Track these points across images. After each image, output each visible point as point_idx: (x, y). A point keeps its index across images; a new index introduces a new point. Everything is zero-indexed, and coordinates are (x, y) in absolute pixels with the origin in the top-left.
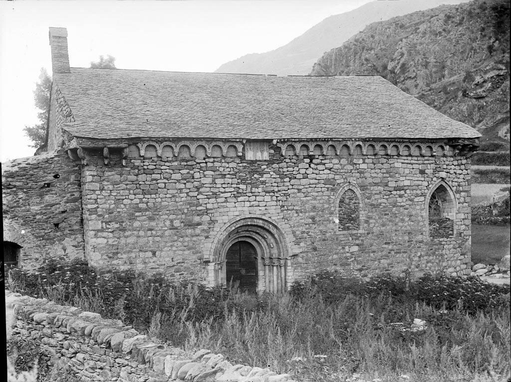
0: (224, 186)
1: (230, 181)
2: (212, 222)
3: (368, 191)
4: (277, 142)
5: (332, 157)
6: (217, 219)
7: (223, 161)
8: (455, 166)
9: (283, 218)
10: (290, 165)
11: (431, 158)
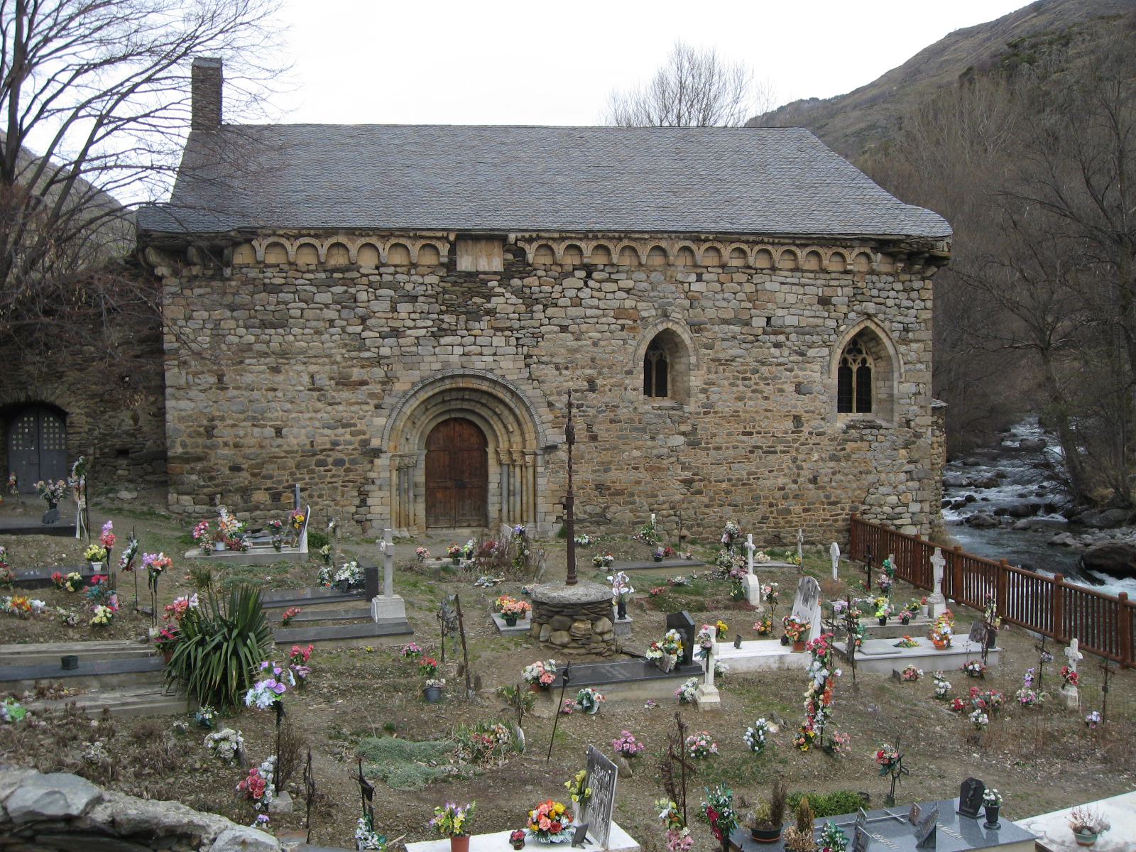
0: (413, 316)
1: (426, 308)
2: (388, 381)
3: (706, 333)
4: (517, 240)
5: (633, 269)
7: (413, 271)
8: (897, 292)
9: (528, 379)
10: (546, 281)
11: (843, 276)
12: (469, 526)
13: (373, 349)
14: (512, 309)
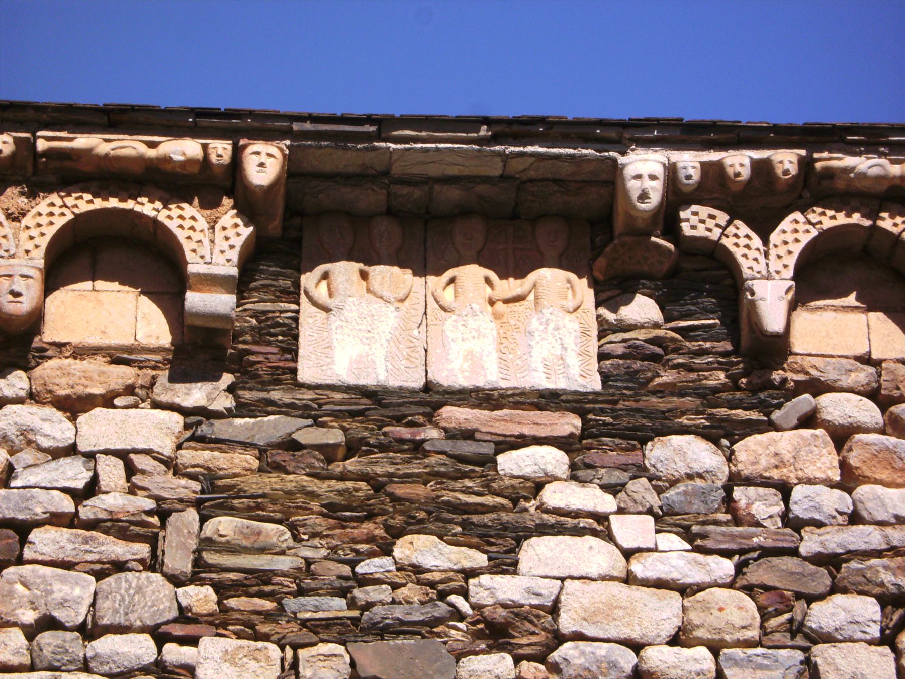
4: (677, 195)
14: (666, 612)
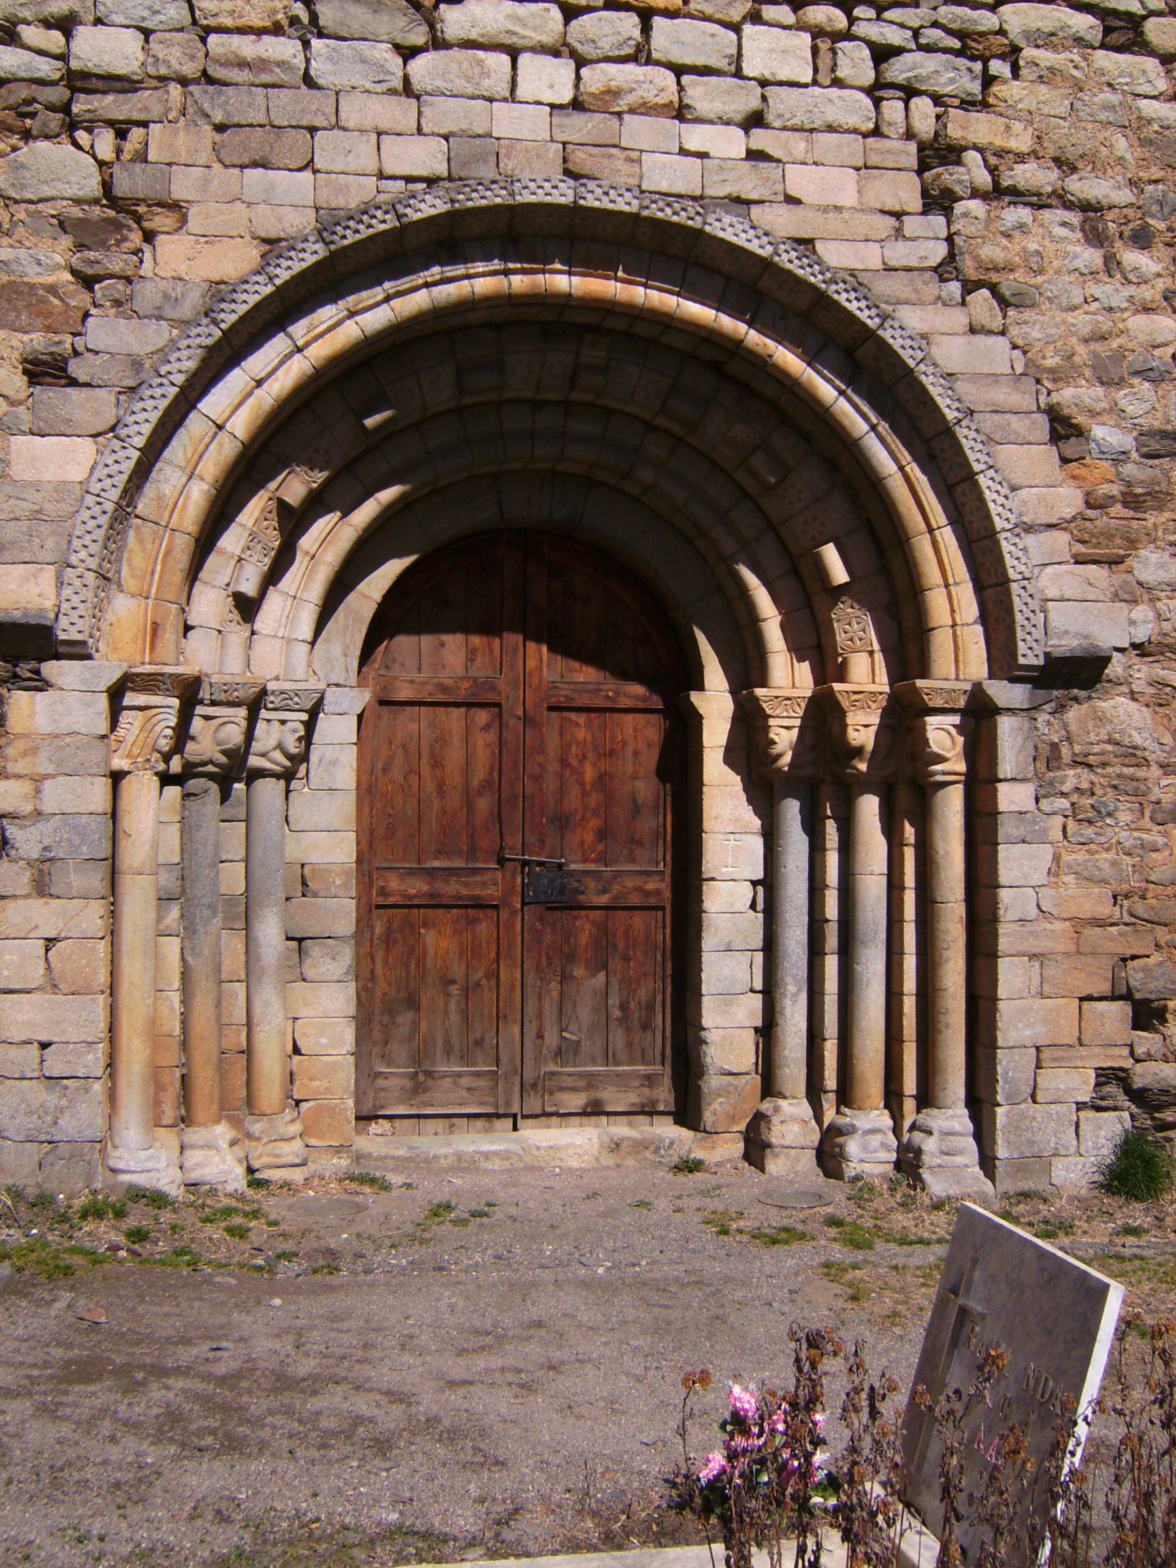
6: (181, 187)
9: (946, 269)
12: (594, 1110)
13: (31, 34)
